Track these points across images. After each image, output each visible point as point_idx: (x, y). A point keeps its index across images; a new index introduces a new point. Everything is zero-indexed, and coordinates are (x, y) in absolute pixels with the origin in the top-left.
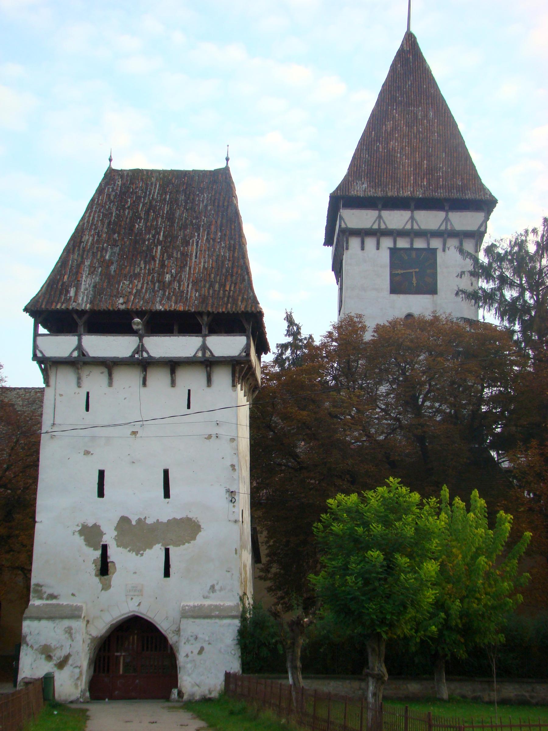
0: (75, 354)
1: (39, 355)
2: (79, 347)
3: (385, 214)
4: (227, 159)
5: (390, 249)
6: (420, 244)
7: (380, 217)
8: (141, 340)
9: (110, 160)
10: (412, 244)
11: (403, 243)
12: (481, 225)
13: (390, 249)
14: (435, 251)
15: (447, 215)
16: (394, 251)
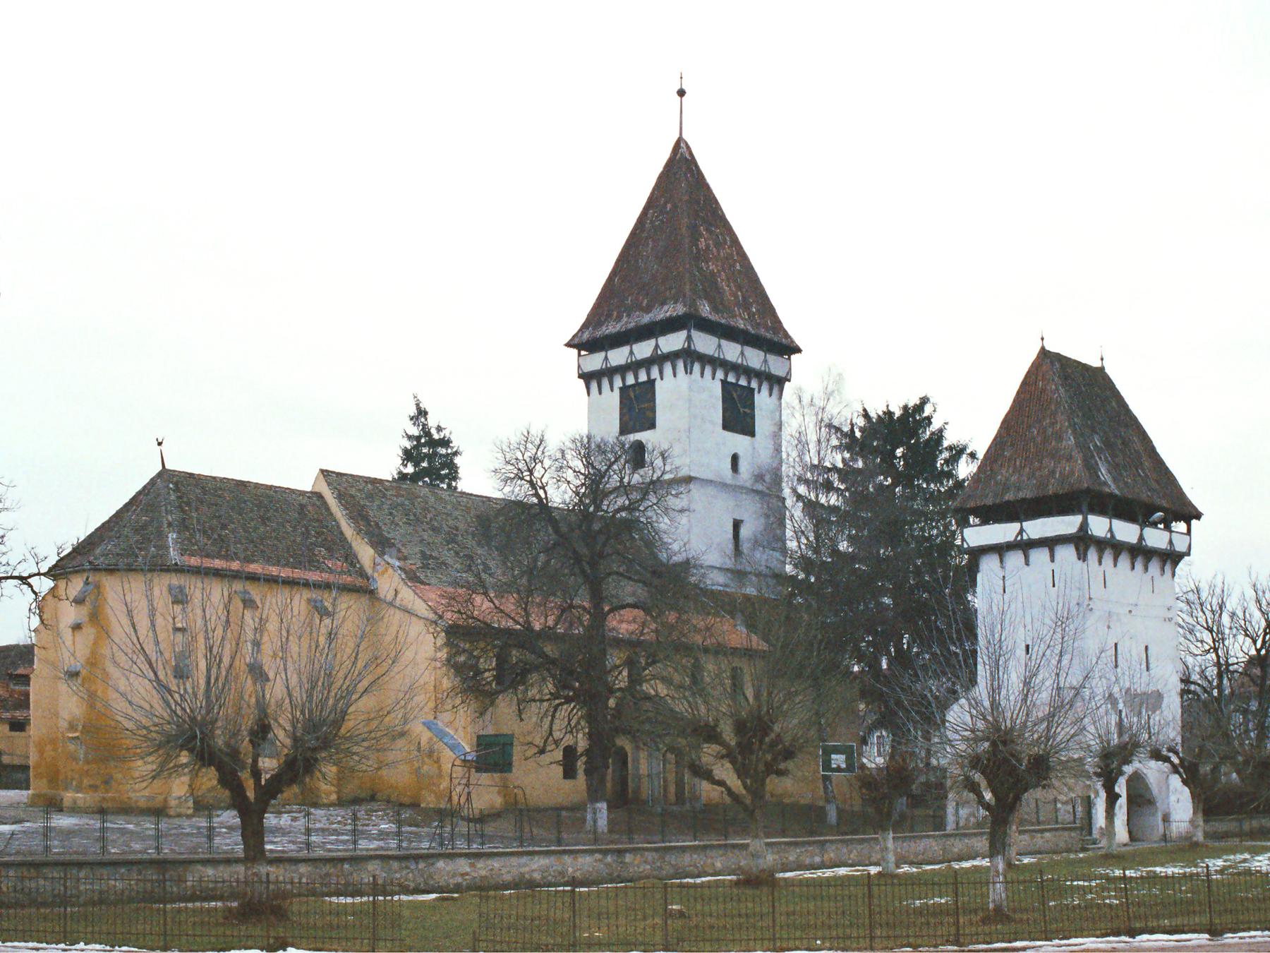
0: (1109, 536)
1: (1090, 533)
2: (1110, 530)
3: (724, 342)
4: (1102, 359)
5: (721, 380)
6: (743, 382)
7: (719, 346)
8: (1142, 530)
9: (1042, 339)
10: (738, 380)
11: (731, 379)
12: (788, 373)
13: (721, 380)
14: (753, 389)
15: (765, 356)
16: (724, 383)
